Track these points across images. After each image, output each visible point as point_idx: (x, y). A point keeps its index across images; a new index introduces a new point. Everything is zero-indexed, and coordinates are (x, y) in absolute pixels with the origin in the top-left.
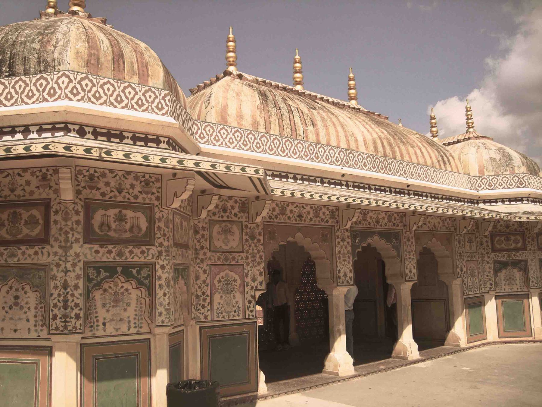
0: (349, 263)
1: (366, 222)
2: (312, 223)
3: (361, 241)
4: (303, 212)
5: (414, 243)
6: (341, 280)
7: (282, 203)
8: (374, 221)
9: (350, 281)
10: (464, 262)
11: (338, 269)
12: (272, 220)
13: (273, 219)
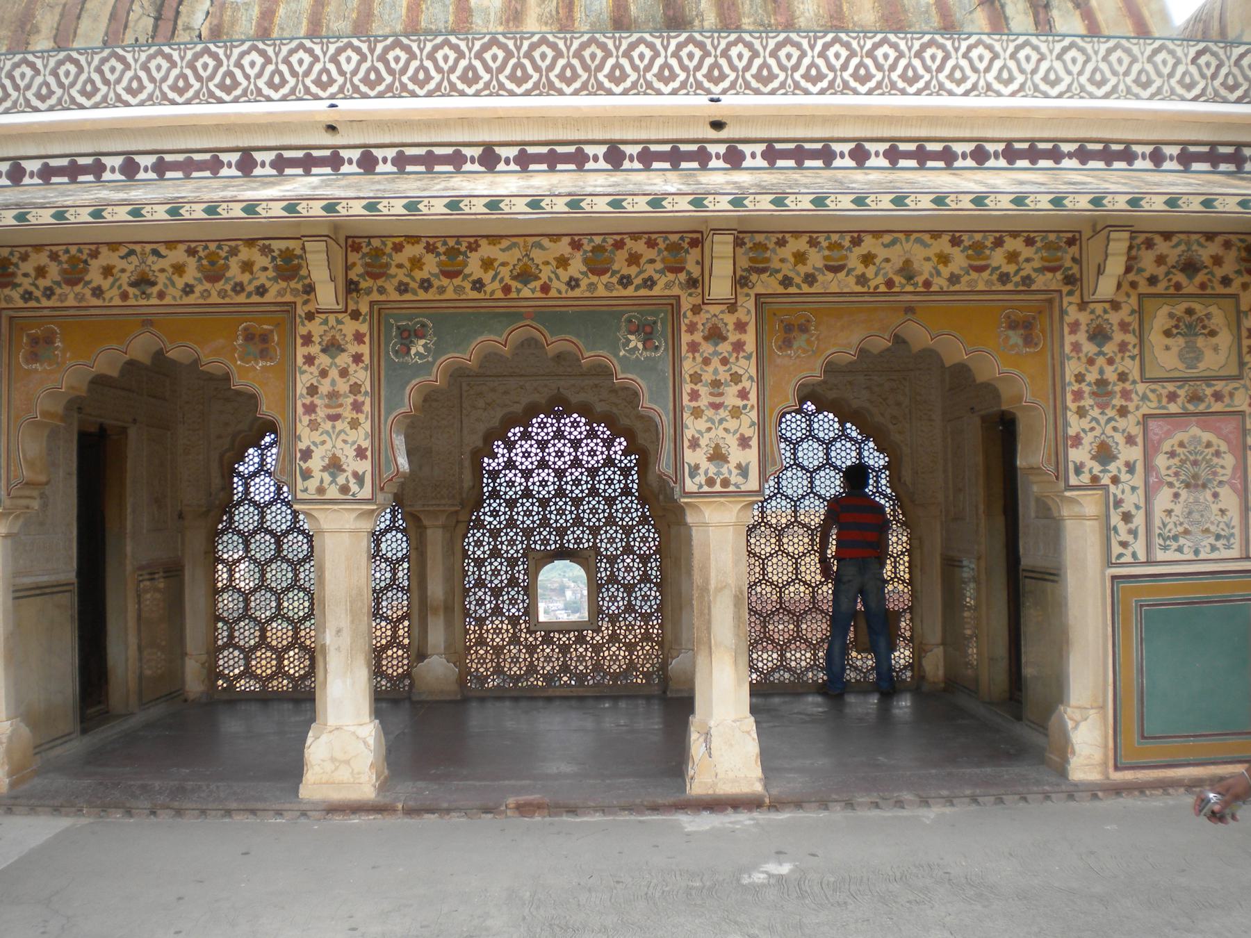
0: (354, 424)
1: (457, 281)
2: (191, 299)
3: (438, 350)
4: (155, 267)
5: (750, 346)
6: (313, 484)
7: (73, 250)
8: (505, 272)
9: (354, 488)
10: (1130, 423)
11: (302, 445)
12: (33, 304)
13: (37, 300)
